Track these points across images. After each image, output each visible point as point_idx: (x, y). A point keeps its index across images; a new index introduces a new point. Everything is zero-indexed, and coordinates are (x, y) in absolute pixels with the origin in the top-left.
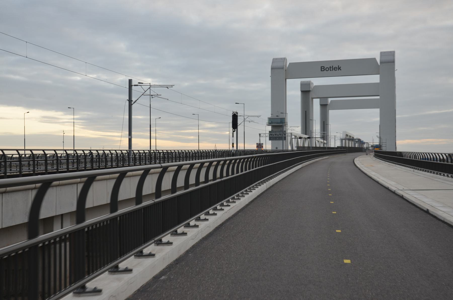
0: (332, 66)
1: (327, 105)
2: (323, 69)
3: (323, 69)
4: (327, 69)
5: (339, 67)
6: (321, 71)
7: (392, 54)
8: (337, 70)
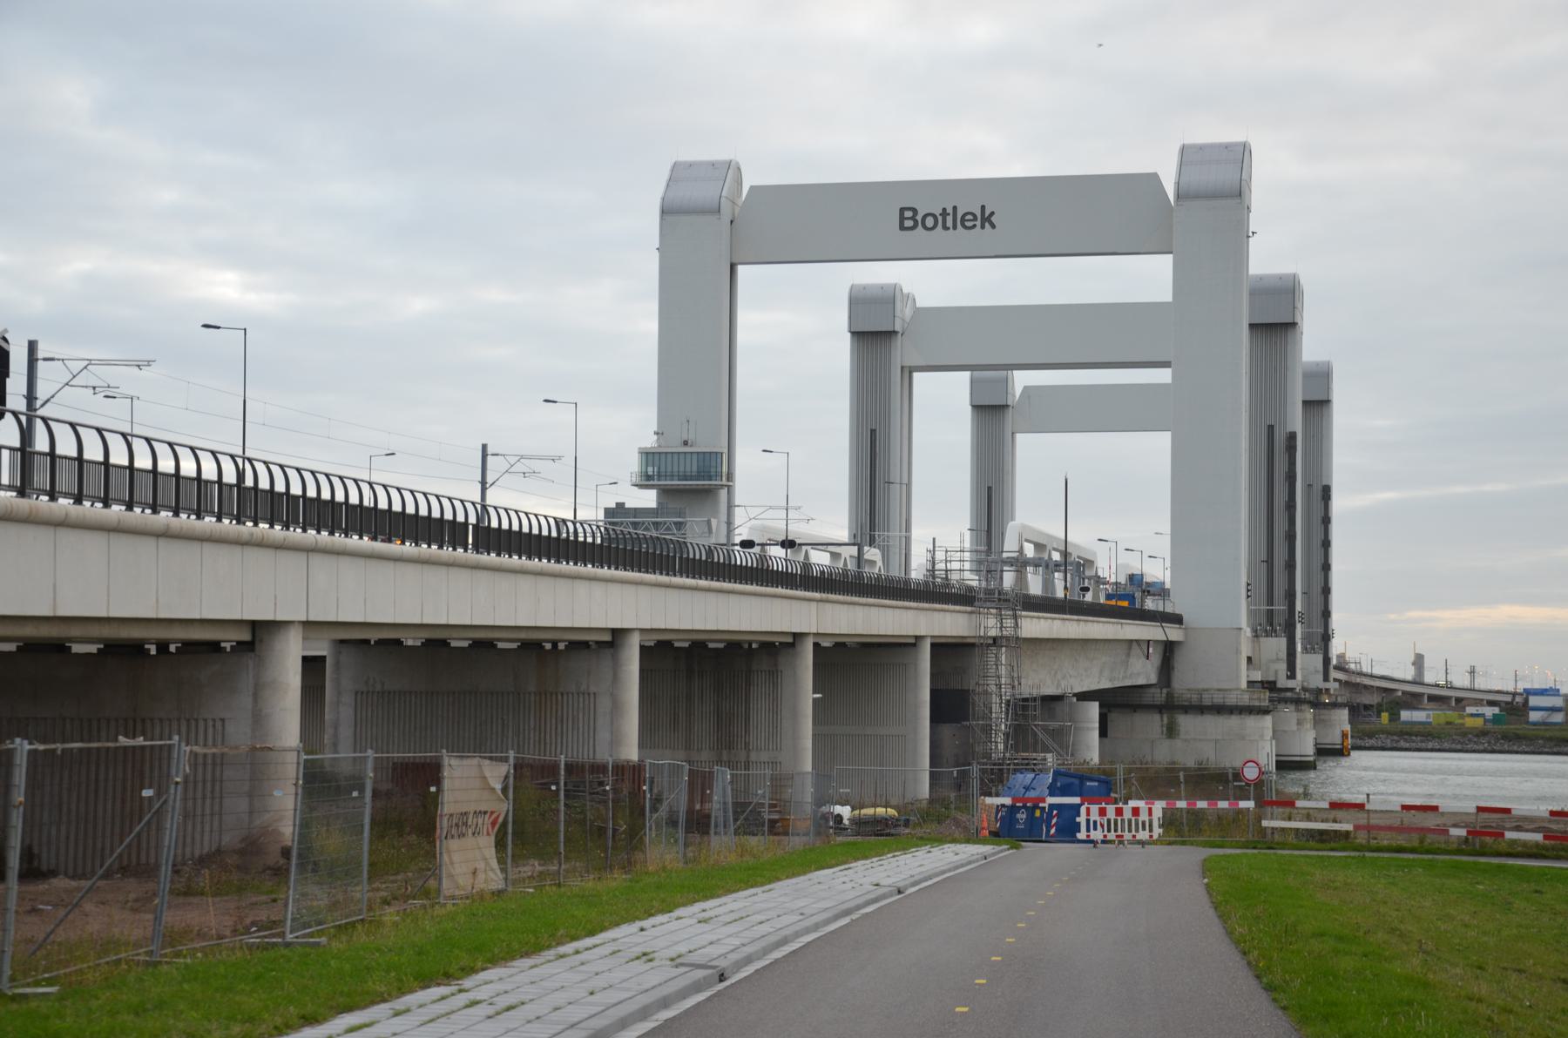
0: (955, 208)
1: (1002, 408)
2: (909, 219)
3: (909, 219)
4: (930, 222)
5: (987, 215)
6: (902, 228)
7: (1240, 154)
8: (975, 226)
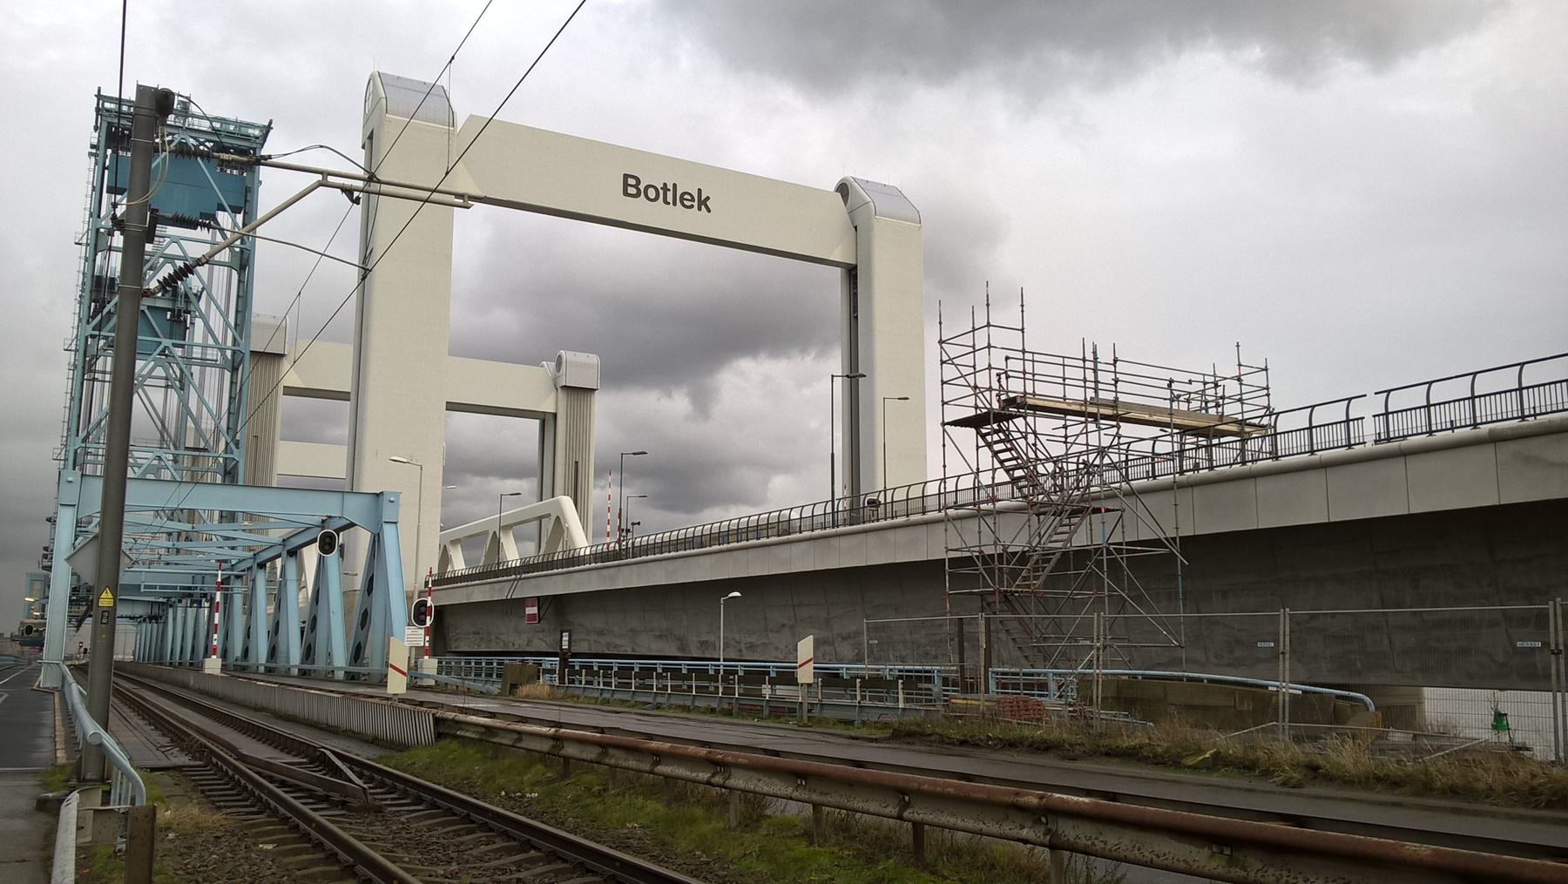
0: (675, 185)
2: (631, 186)
6: (626, 193)
8: (692, 206)
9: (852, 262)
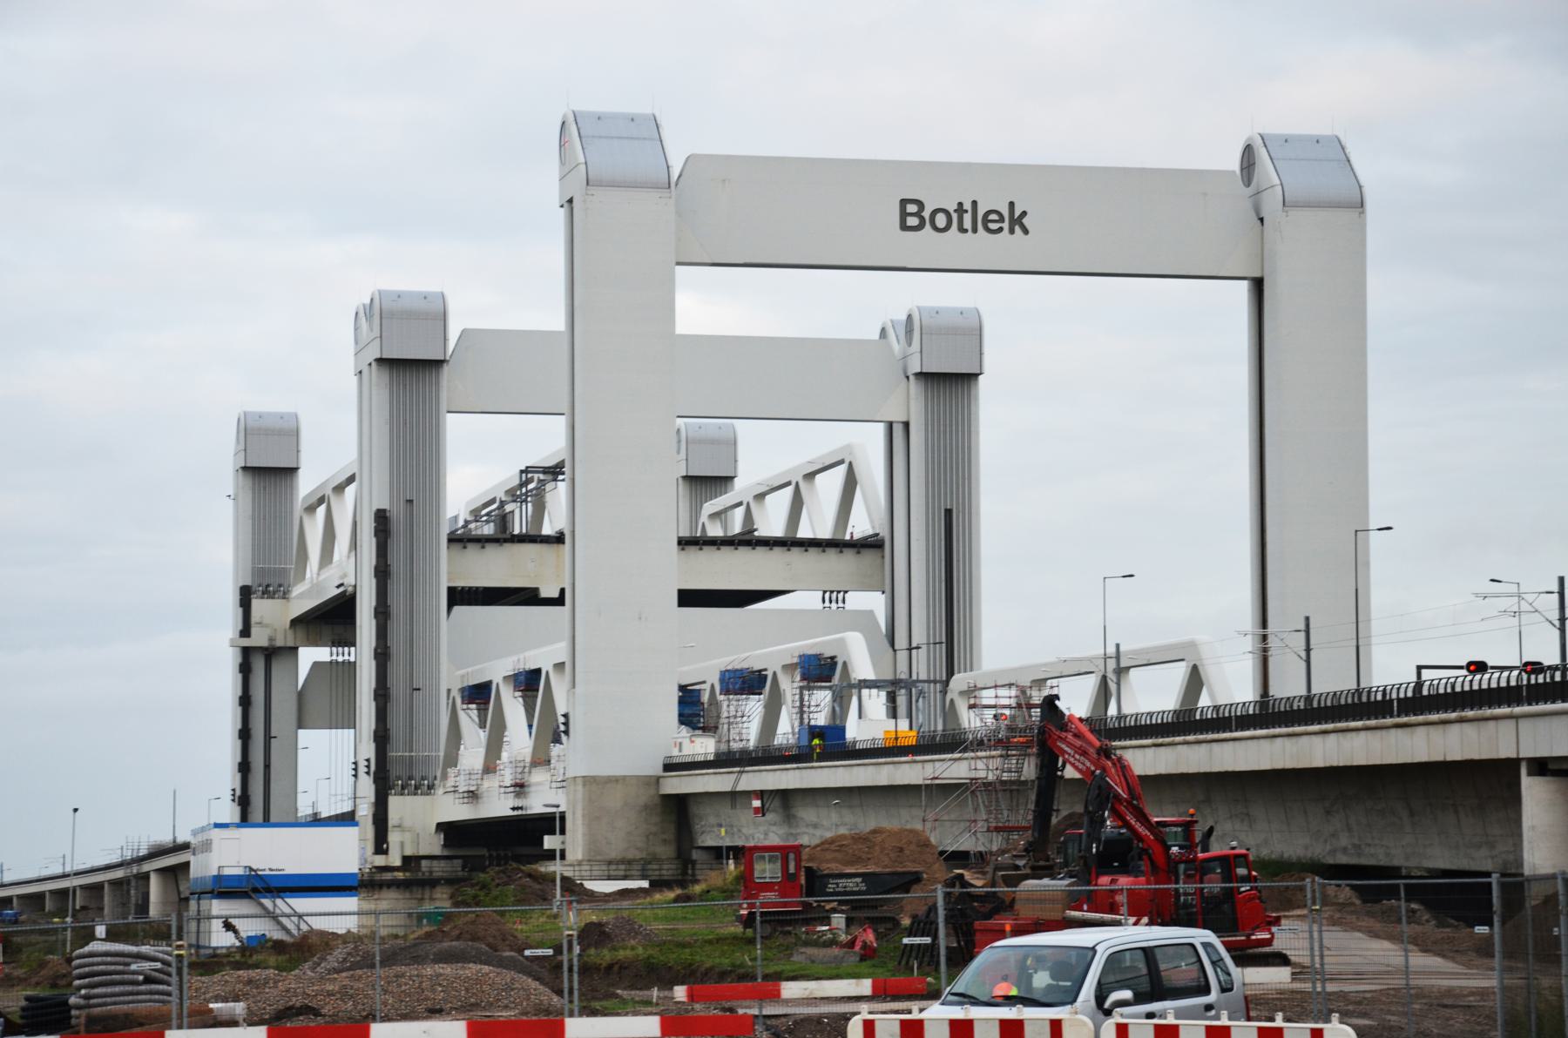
0: (974, 203)
2: (912, 215)
3: (912, 215)
4: (941, 220)
5: (1016, 216)
6: (904, 227)
8: (1001, 229)
9: (1257, 275)
